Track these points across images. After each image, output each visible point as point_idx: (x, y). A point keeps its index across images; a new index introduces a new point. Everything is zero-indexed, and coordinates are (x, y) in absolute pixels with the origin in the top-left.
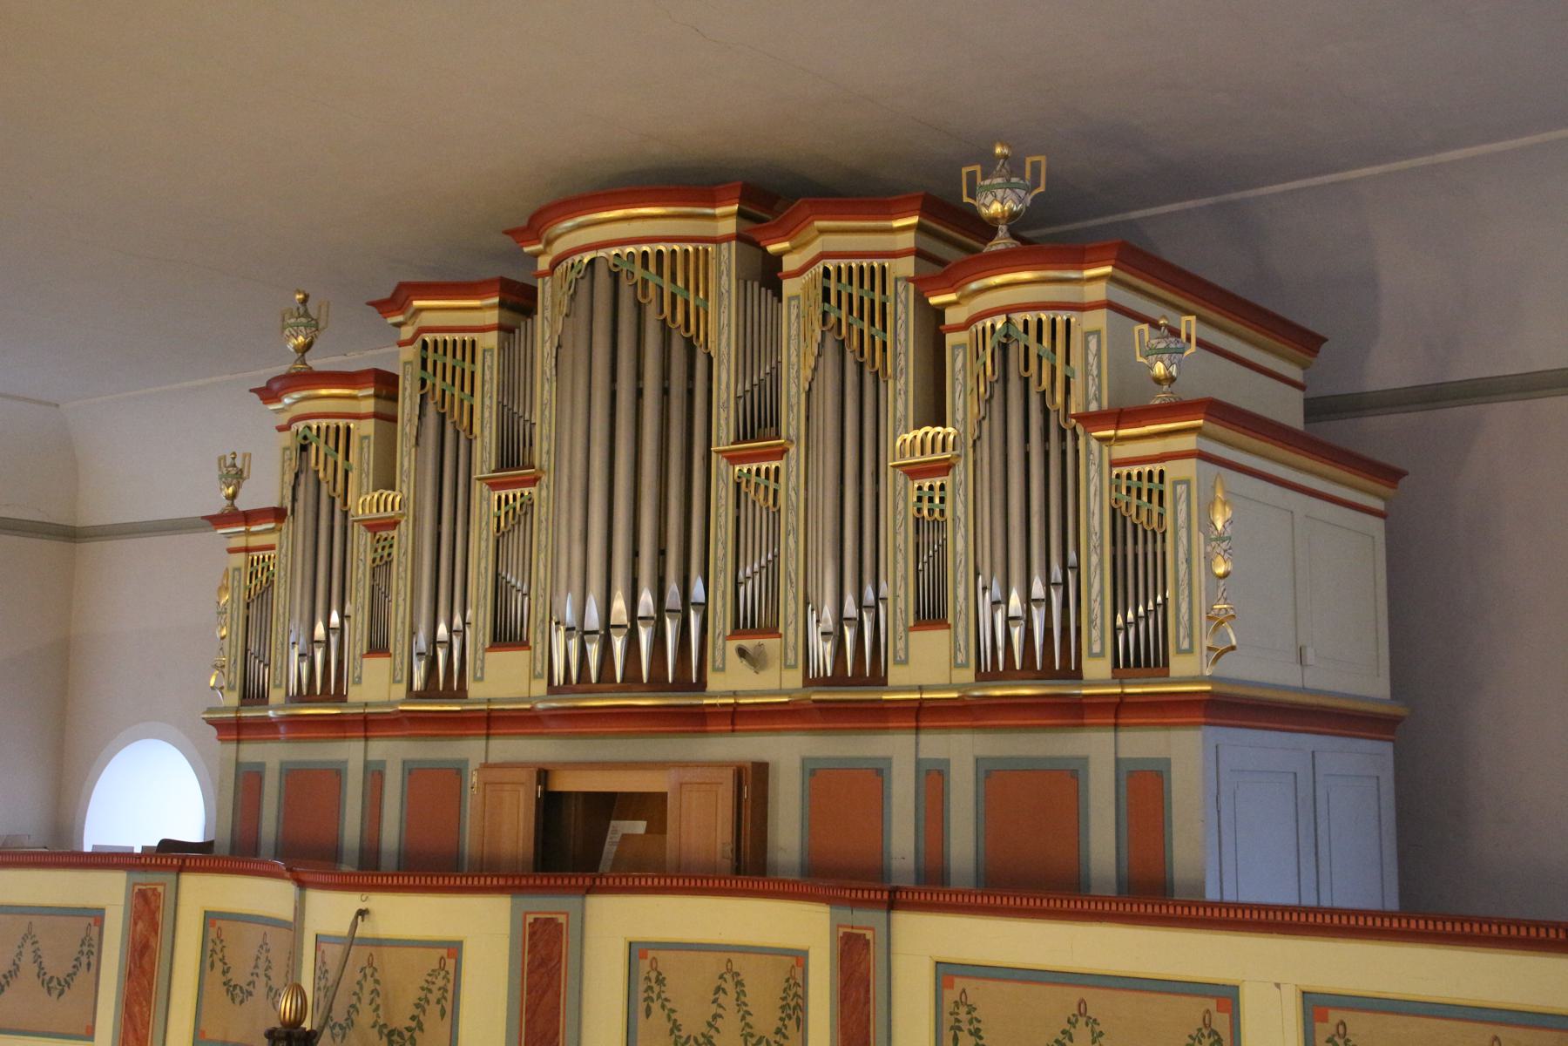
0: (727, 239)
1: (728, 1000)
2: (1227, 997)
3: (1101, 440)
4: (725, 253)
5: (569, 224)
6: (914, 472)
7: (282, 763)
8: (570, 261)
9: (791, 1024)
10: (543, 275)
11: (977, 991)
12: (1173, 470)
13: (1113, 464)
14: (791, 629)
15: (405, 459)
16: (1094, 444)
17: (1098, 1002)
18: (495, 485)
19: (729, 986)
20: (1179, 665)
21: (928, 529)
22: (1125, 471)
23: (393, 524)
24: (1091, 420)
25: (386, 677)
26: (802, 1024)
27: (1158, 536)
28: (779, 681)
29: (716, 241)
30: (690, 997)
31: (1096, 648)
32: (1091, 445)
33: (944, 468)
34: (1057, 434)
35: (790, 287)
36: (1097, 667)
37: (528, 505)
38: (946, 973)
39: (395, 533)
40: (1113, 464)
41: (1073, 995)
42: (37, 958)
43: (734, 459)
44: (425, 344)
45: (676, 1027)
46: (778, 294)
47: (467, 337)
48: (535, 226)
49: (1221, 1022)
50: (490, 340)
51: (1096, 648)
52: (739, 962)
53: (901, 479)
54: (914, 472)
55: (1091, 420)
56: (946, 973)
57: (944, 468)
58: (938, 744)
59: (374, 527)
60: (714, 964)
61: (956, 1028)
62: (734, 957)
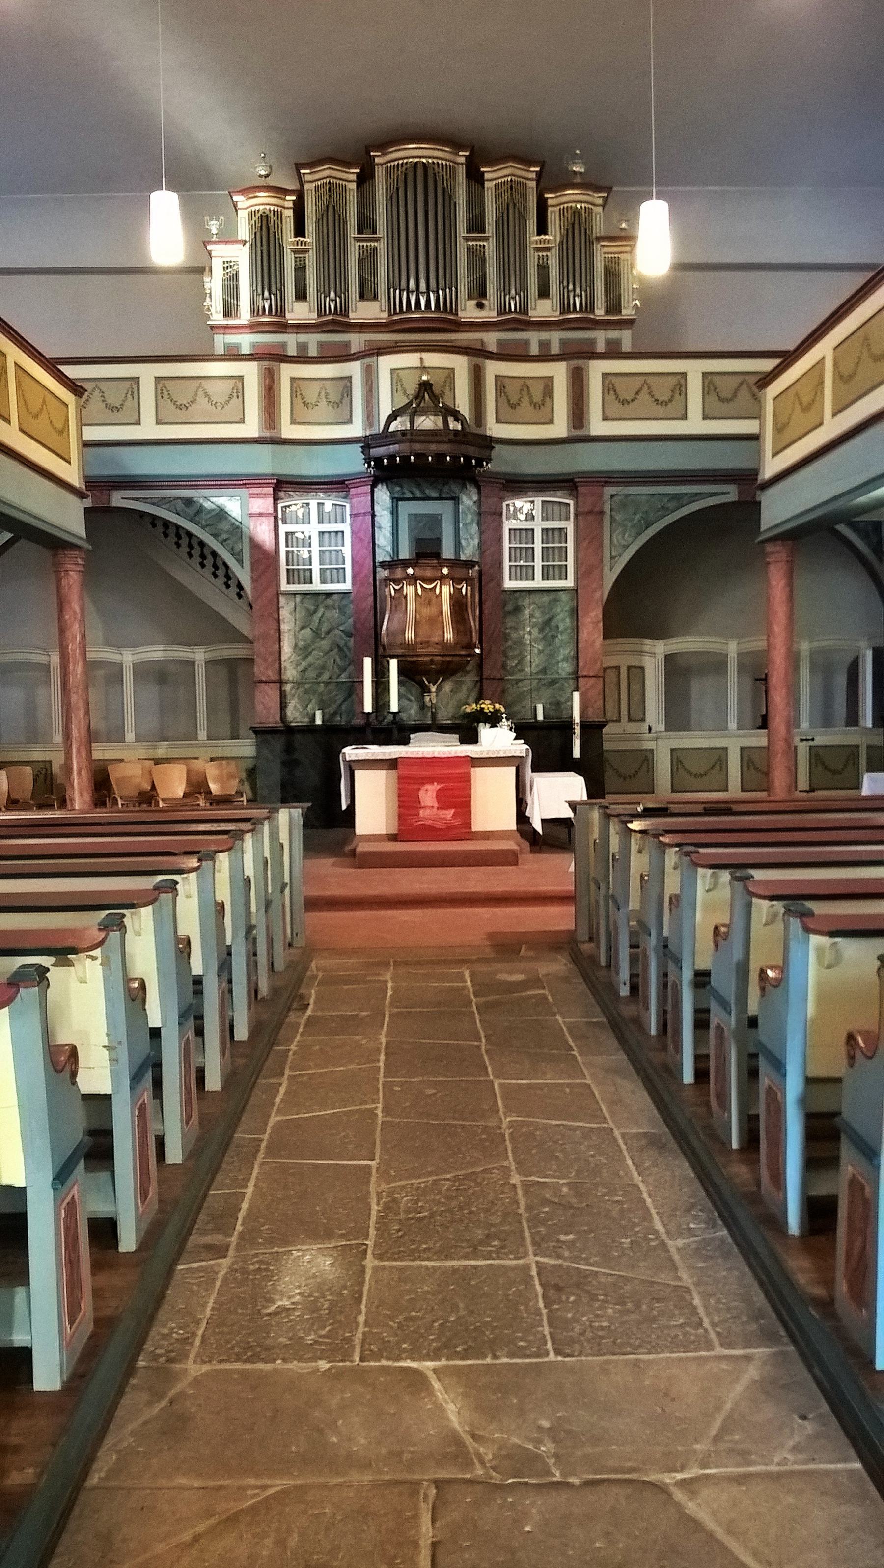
0: (462, 164)
1: (525, 394)
2: (684, 375)
3: (604, 246)
4: (460, 169)
5: (394, 149)
6: (538, 250)
7: (250, 343)
8: (405, 161)
9: (548, 398)
10: (378, 165)
11: (614, 379)
12: (622, 256)
13: (605, 253)
14: (492, 298)
15: (310, 226)
16: (599, 246)
17: (650, 379)
18: (358, 240)
19: (525, 389)
20: (624, 312)
21: (543, 270)
22: (606, 256)
23: (306, 251)
24: (599, 239)
25: (307, 309)
26: (551, 396)
27: (619, 275)
28: (490, 314)
29: (458, 164)
30: (512, 390)
31: (600, 306)
32: (597, 246)
33: (548, 249)
34: (590, 242)
35: (487, 184)
36: (600, 312)
37: (375, 249)
38: (605, 375)
39: (307, 256)
40: (605, 253)
41: (643, 378)
42: (207, 395)
43: (467, 239)
44: (329, 182)
45: (509, 401)
46: (483, 187)
47: (344, 183)
48: (383, 146)
49: (683, 382)
50: (353, 186)
51: (600, 306)
52: (529, 382)
53: (532, 252)
54: (538, 250)
55: (599, 239)
56: (605, 375)
57: (548, 249)
58: (544, 335)
59: (295, 251)
60: (521, 382)
61: (609, 390)
62: (526, 380)
